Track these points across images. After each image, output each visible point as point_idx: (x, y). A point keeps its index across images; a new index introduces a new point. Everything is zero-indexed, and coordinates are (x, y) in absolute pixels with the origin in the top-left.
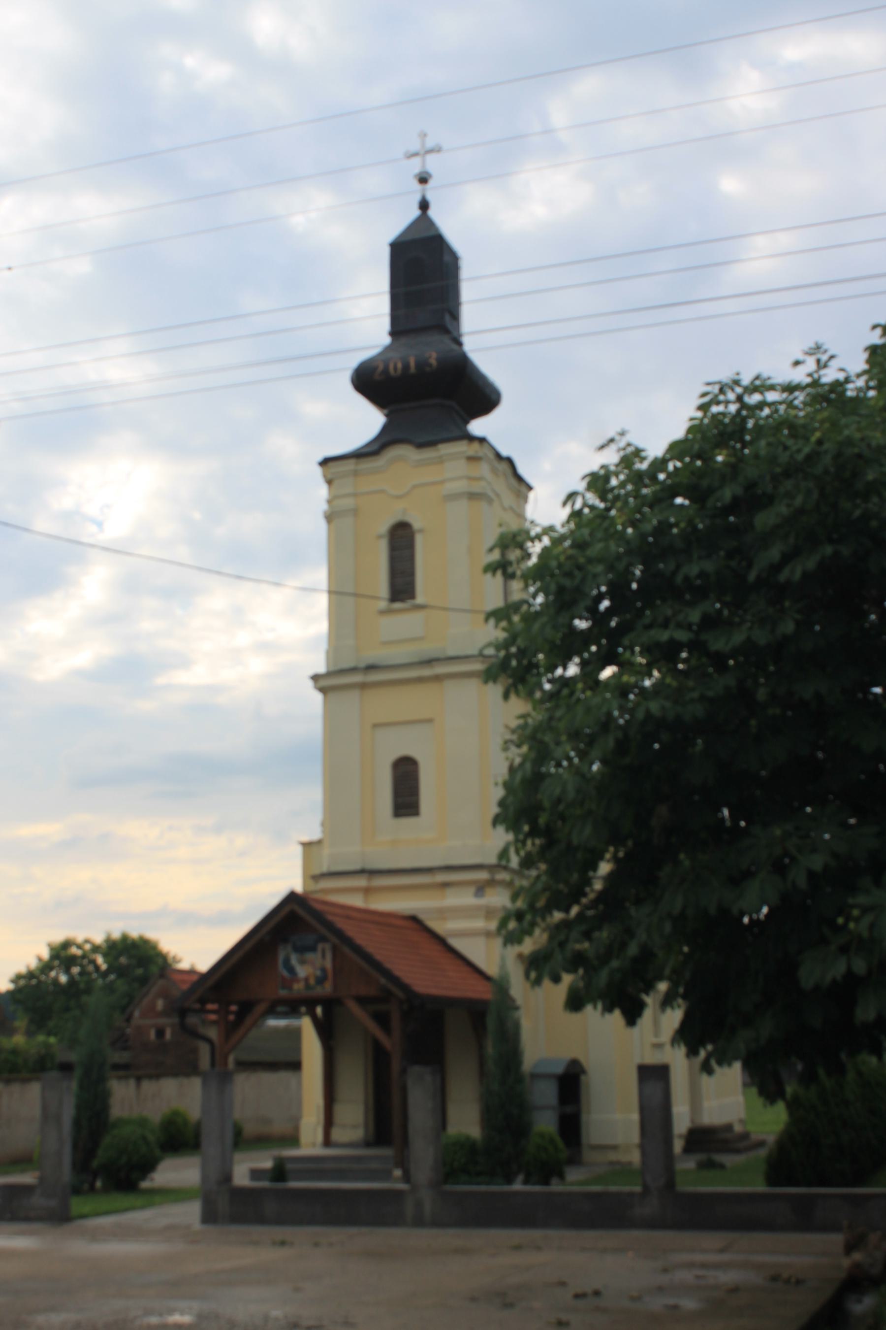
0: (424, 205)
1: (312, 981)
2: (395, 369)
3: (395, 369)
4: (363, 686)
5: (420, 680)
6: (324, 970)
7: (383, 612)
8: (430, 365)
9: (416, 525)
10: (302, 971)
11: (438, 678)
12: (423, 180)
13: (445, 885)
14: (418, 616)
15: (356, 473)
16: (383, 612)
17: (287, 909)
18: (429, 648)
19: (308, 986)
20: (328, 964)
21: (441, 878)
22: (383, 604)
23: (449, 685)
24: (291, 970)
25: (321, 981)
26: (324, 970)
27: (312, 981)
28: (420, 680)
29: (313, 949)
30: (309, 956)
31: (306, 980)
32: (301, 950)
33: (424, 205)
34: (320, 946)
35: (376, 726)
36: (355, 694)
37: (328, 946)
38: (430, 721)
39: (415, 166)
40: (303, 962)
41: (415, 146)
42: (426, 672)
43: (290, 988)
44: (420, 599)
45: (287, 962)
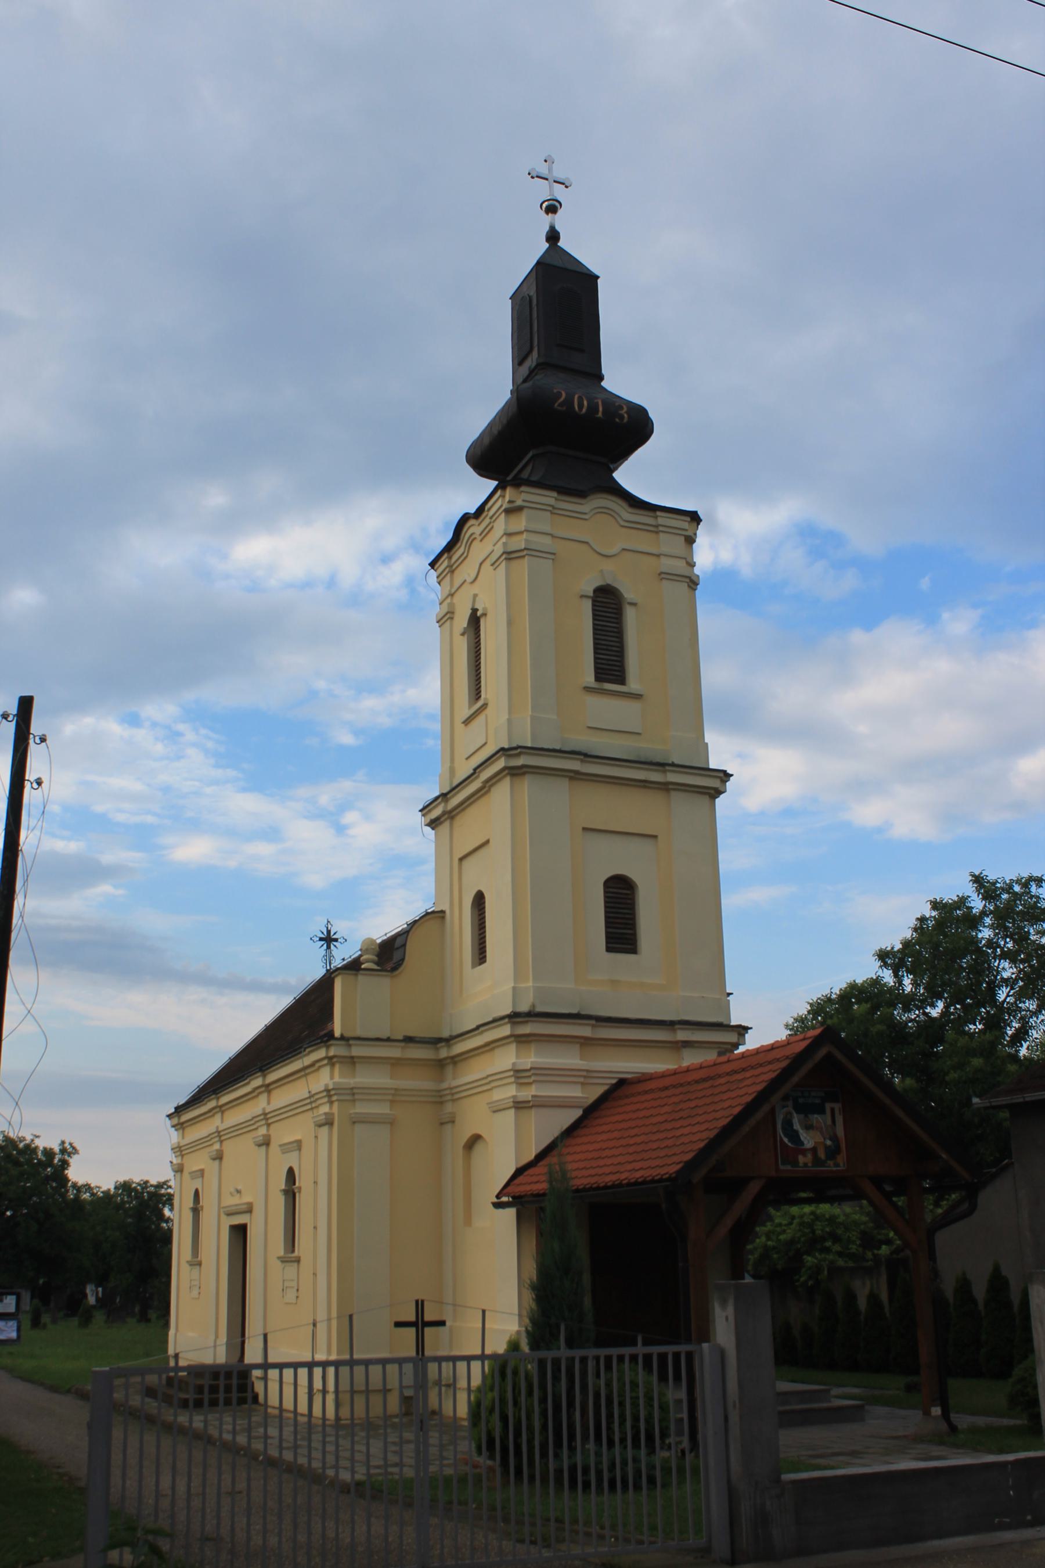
0: (553, 236)
1: (822, 1155)
2: (581, 406)
3: (581, 406)
4: (575, 776)
5: (644, 784)
6: (834, 1138)
7: (588, 689)
8: (622, 417)
9: (628, 594)
10: (808, 1140)
11: (666, 787)
12: (552, 209)
13: (687, 1044)
14: (634, 706)
15: (553, 510)
16: (588, 689)
17: (823, 1052)
18: (649, 747)
19: (817, 1161)
20: (840, 1131)
21: (682, 1035)
22: (590, 678)
23: (676, 797)
24: (795, 1137)
25: (833, 1153)
26: (834, 1138)
27: (822, 1155)
28: (644, 784)
29: (821, 1111)
30: (815, 1118)
31: (814, 1150)
32: (805, 1109)
33: (553, 236)
34: (828, 1106)
35: (584, 829)
36: (564, 784)
37: (837, 1106)
38: (655, 837)
39: (542, 191)
40: (808, 1127)
41: (543, 170)
42: (655, 776)
43: (795, 1163)
44: (633, 684)
45: (788, 1124)
